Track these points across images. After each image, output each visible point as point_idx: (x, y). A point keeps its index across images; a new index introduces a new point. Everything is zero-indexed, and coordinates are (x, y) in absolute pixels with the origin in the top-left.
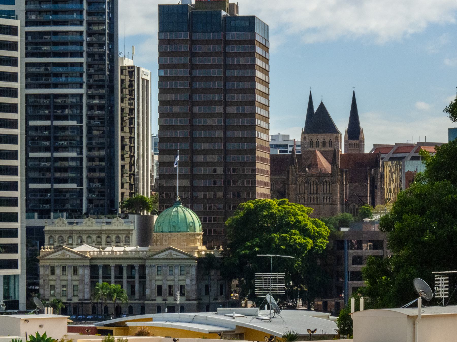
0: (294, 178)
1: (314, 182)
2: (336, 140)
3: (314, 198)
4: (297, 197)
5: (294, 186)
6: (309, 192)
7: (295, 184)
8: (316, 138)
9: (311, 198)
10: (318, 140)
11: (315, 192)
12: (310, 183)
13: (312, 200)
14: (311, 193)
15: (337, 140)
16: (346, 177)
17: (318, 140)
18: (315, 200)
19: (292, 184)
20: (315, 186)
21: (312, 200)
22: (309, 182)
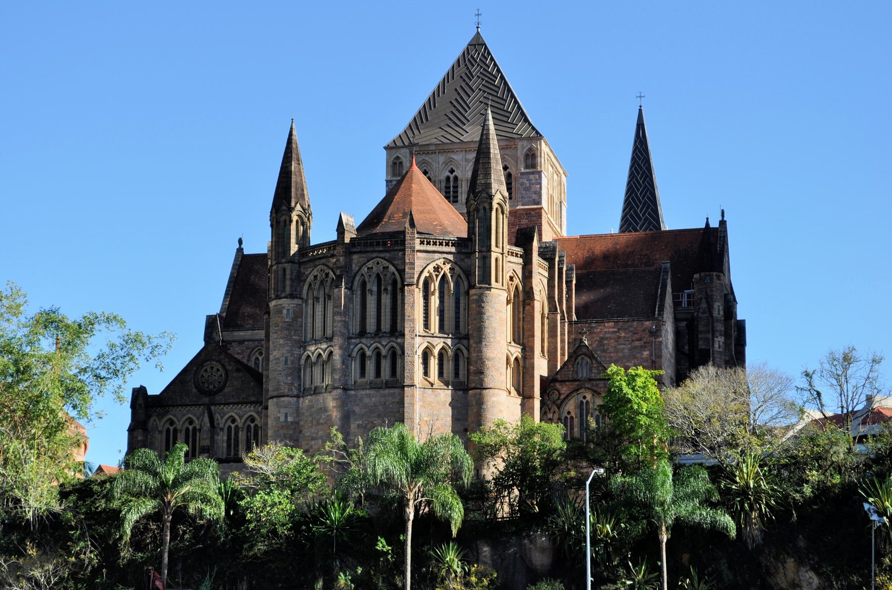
0: (288, 266)
1: (378, 275)
2: (526, 167)
3: (378, 355)
4: (301, 355)
5: (285, 302)
6: (355, 328)
7: (292, 296)
8: (446, 164)
9: (363, 356)
10: (452, 171)
11: (386, 326)
12: (364, 284)
13: (370, 366)
14: (363, 333)
15: (533, 165)
16: (551, 279)
17: (452, 171)
18: (386, 365)
19: (278, 297)
20: (386, 300)
21: (370, 366)
22: (357, 278)
